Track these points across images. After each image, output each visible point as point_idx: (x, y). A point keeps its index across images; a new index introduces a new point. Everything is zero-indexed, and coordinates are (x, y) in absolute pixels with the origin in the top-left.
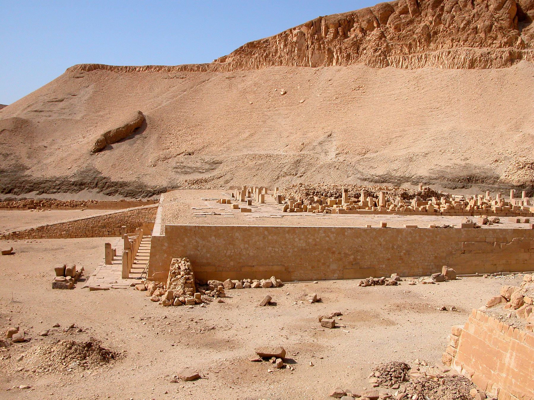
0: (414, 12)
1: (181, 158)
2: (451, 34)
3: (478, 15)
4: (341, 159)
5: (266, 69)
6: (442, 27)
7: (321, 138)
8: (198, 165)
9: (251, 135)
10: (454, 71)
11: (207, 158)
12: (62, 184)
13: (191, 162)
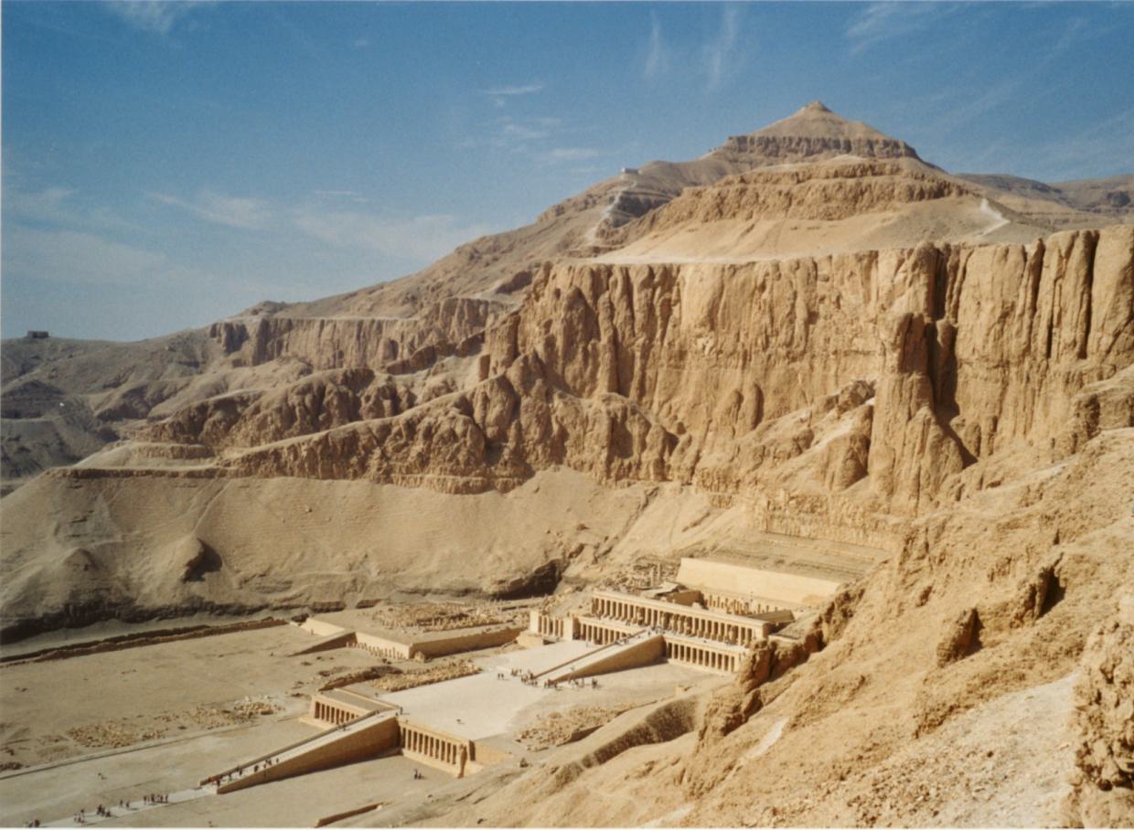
0: (407, 436)
1: (257, 580)
2: (439, 463)
3: (458, 450)
4: (382, 577)
5: (277, 480)
6: (431, 455)
7: (360, 559)
8: (273, 585)
9: (303, 555)
10: (444, 496)
11: (279, 579)
12: (176, 610)
13: (267, 583)
